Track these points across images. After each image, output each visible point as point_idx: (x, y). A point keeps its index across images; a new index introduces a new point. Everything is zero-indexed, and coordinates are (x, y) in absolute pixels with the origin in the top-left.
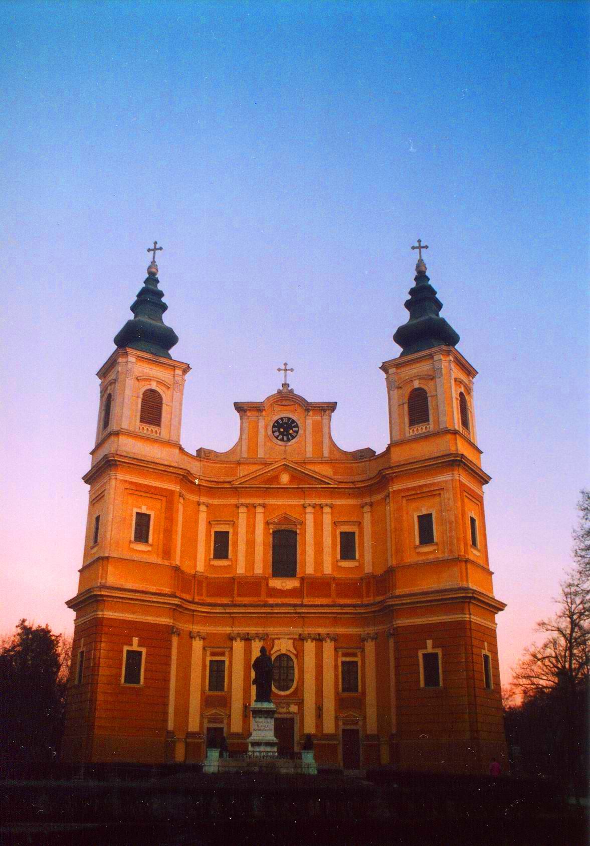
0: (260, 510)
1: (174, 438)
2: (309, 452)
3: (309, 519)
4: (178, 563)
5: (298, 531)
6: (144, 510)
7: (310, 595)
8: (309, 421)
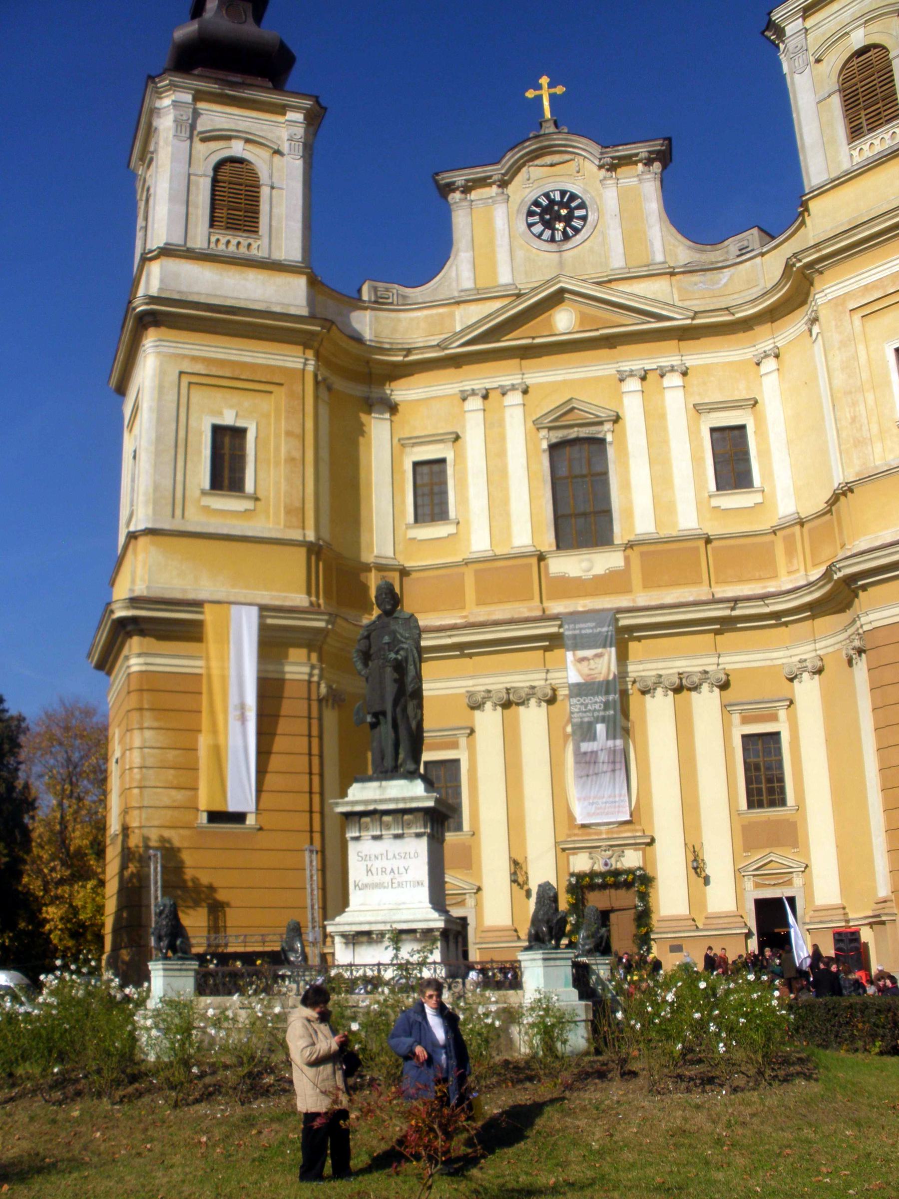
2: (617, 262)
3: (632, 407)
5: (609, 438)
6: (228, 419)
7: (649, 584)
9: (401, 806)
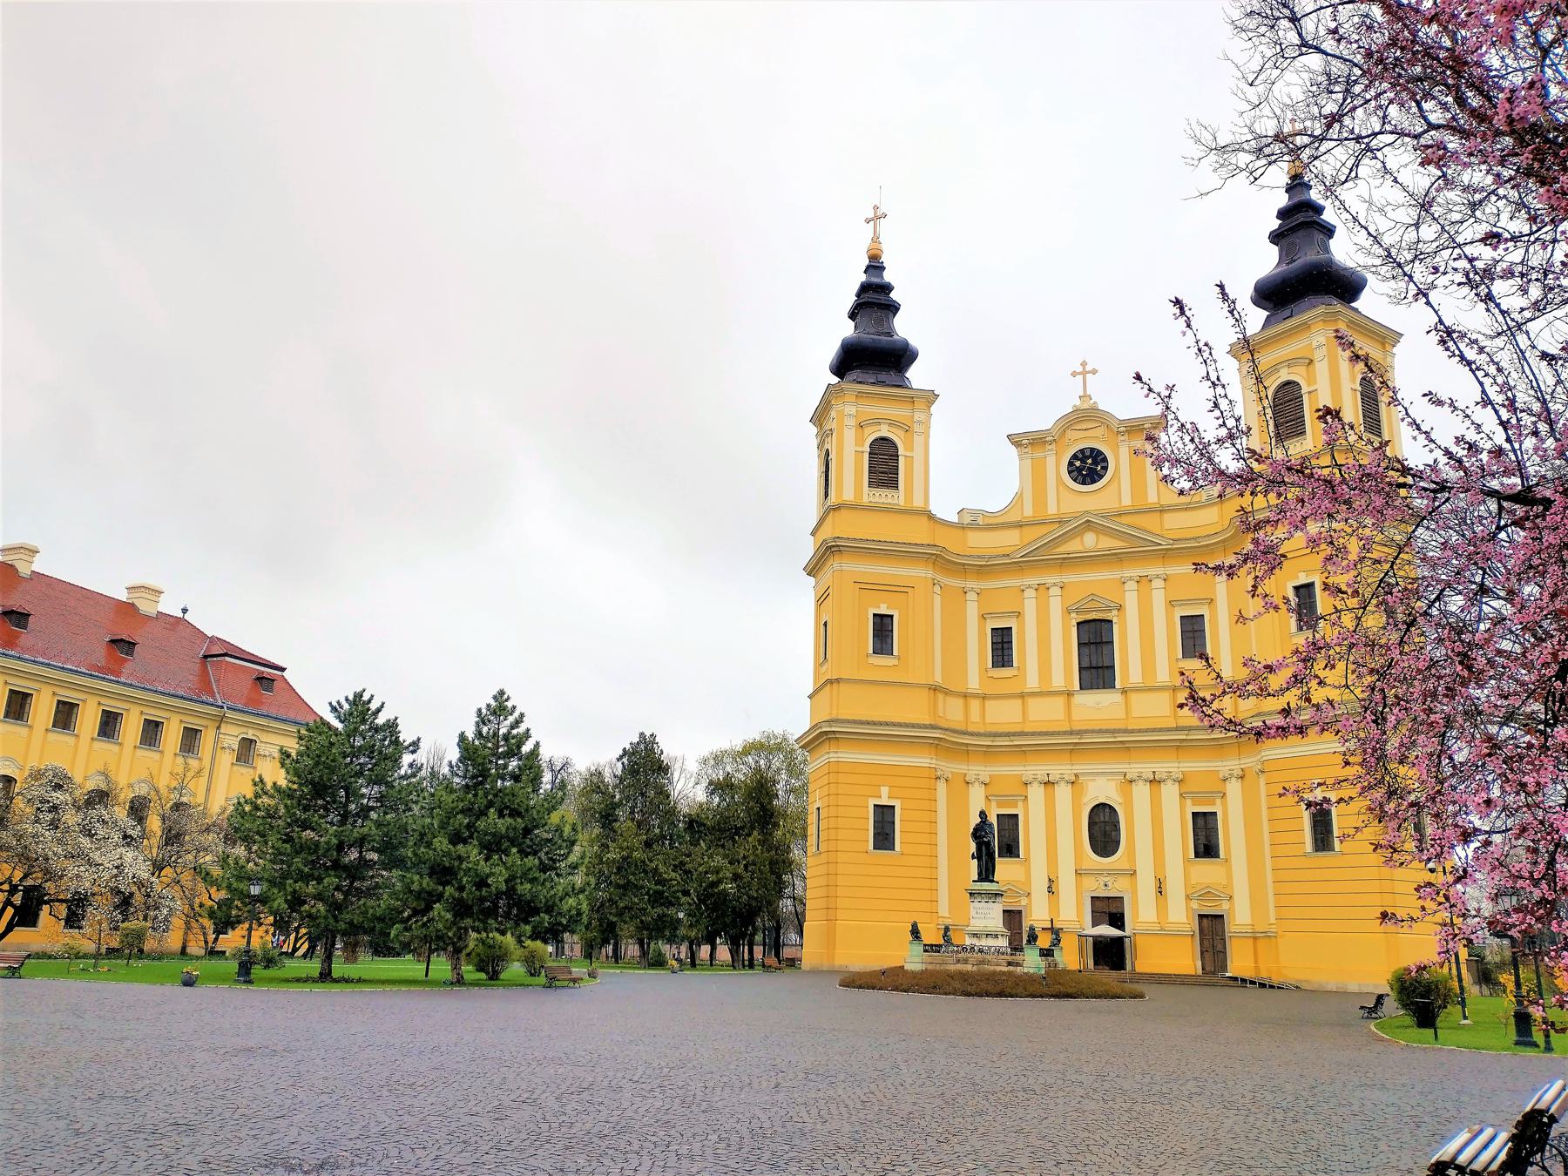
0: (1055, 591)
1: (918, 503)
2: (1127, 501)
3: (1131, 600)
4: (938, 679)
6: (883, 610)
8: (1124, 452)
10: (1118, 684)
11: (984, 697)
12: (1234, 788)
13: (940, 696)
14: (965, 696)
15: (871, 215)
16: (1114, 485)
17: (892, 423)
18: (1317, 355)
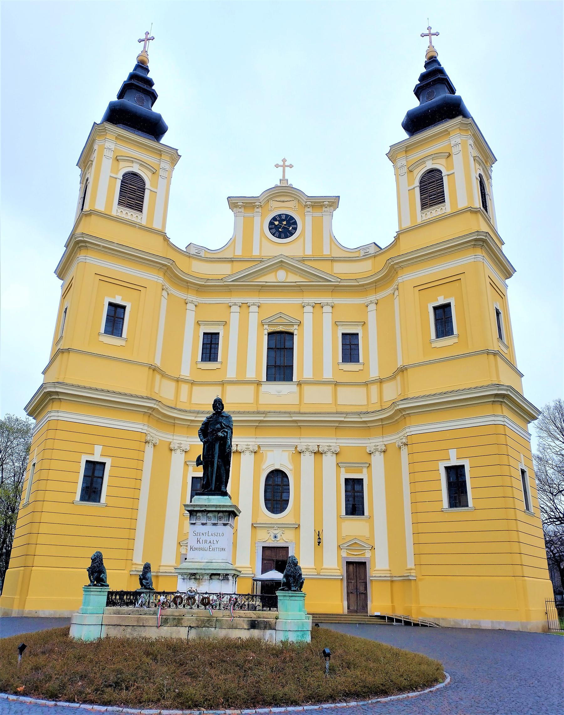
0: (254, 309)
1: (157, 226)
2: (309, 252)
3: (308, 319)
4: (158, 362)
6: (118, 300)
8: (309, 219)
9: (218, 509)
10: (295, 378)
11: (193, 383)
12: (378, 460)
13: (158, 377)
14: (178, 380)
15: (143, 37)
16: (302, 239)
17: (143, 164)
18: (454, 150)
